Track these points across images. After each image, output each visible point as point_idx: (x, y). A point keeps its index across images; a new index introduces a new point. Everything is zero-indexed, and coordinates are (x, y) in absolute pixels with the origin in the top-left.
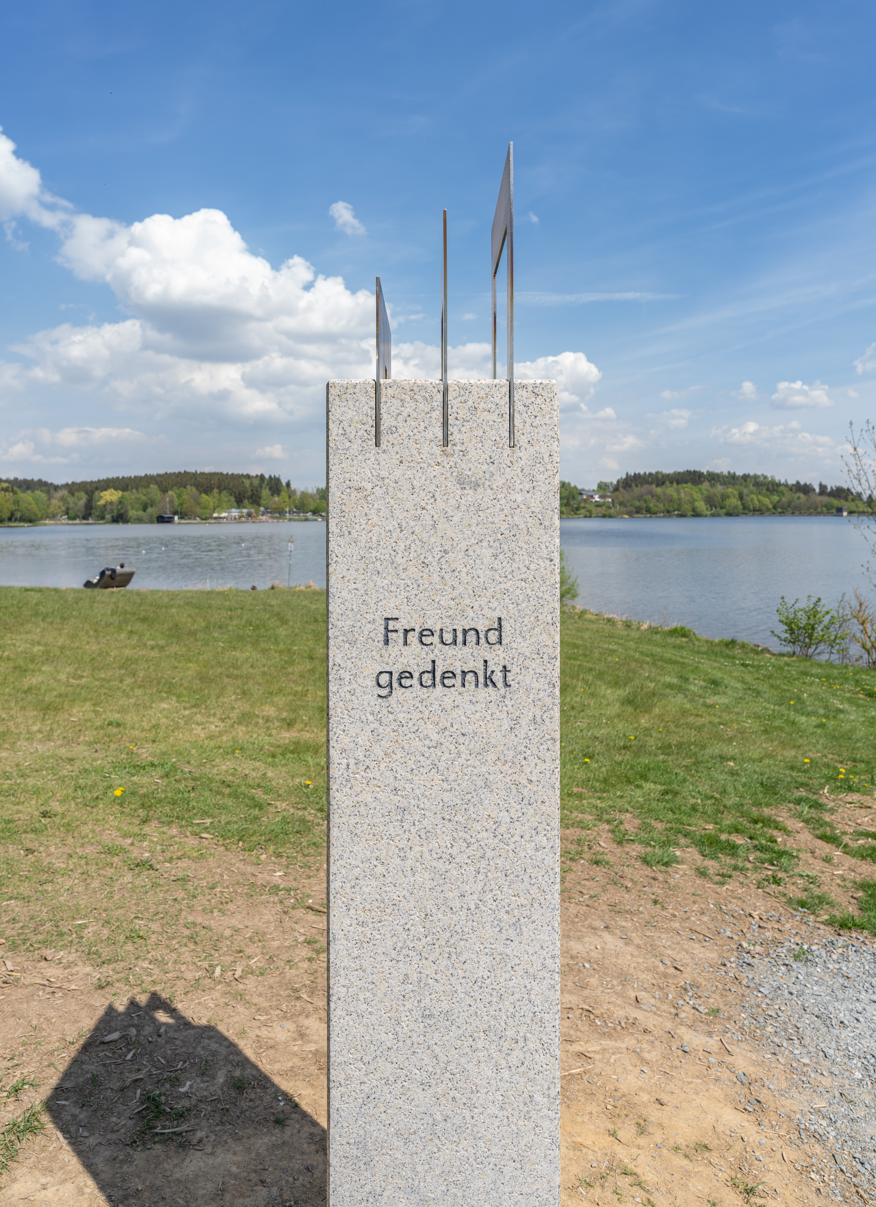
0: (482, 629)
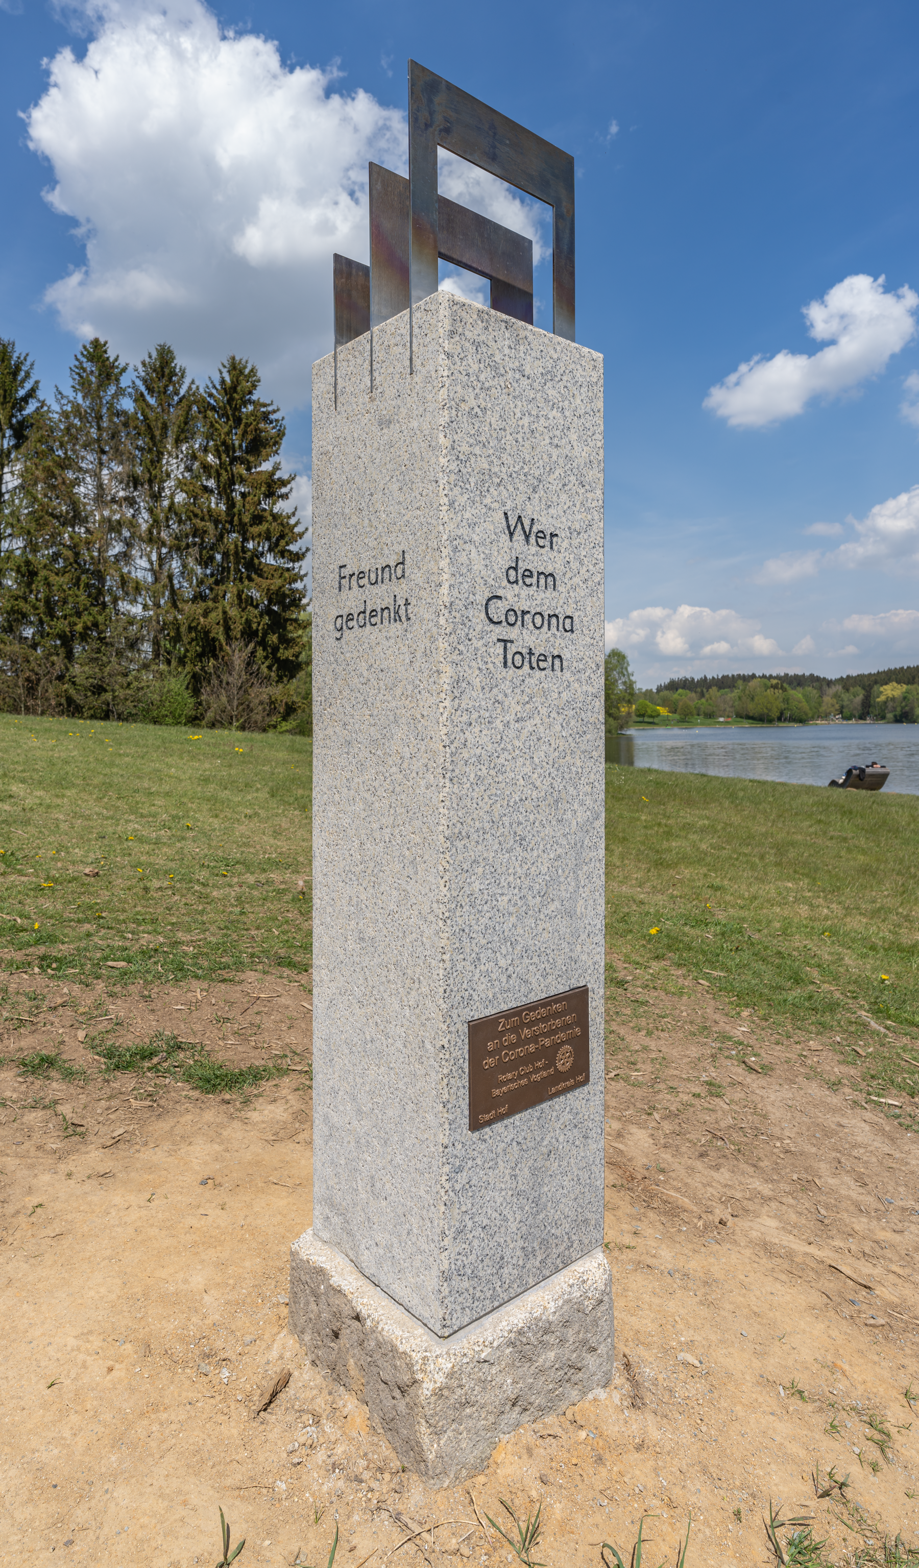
0: (392, 564)
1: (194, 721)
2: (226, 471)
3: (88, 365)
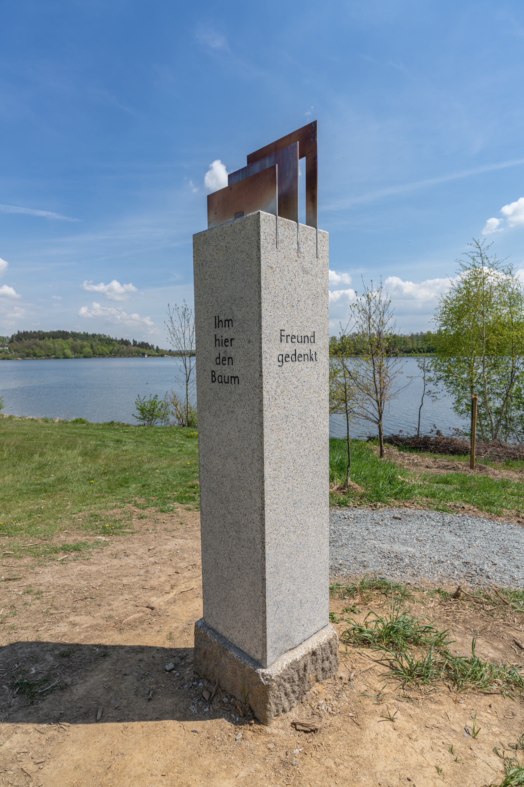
0: (309, 336)
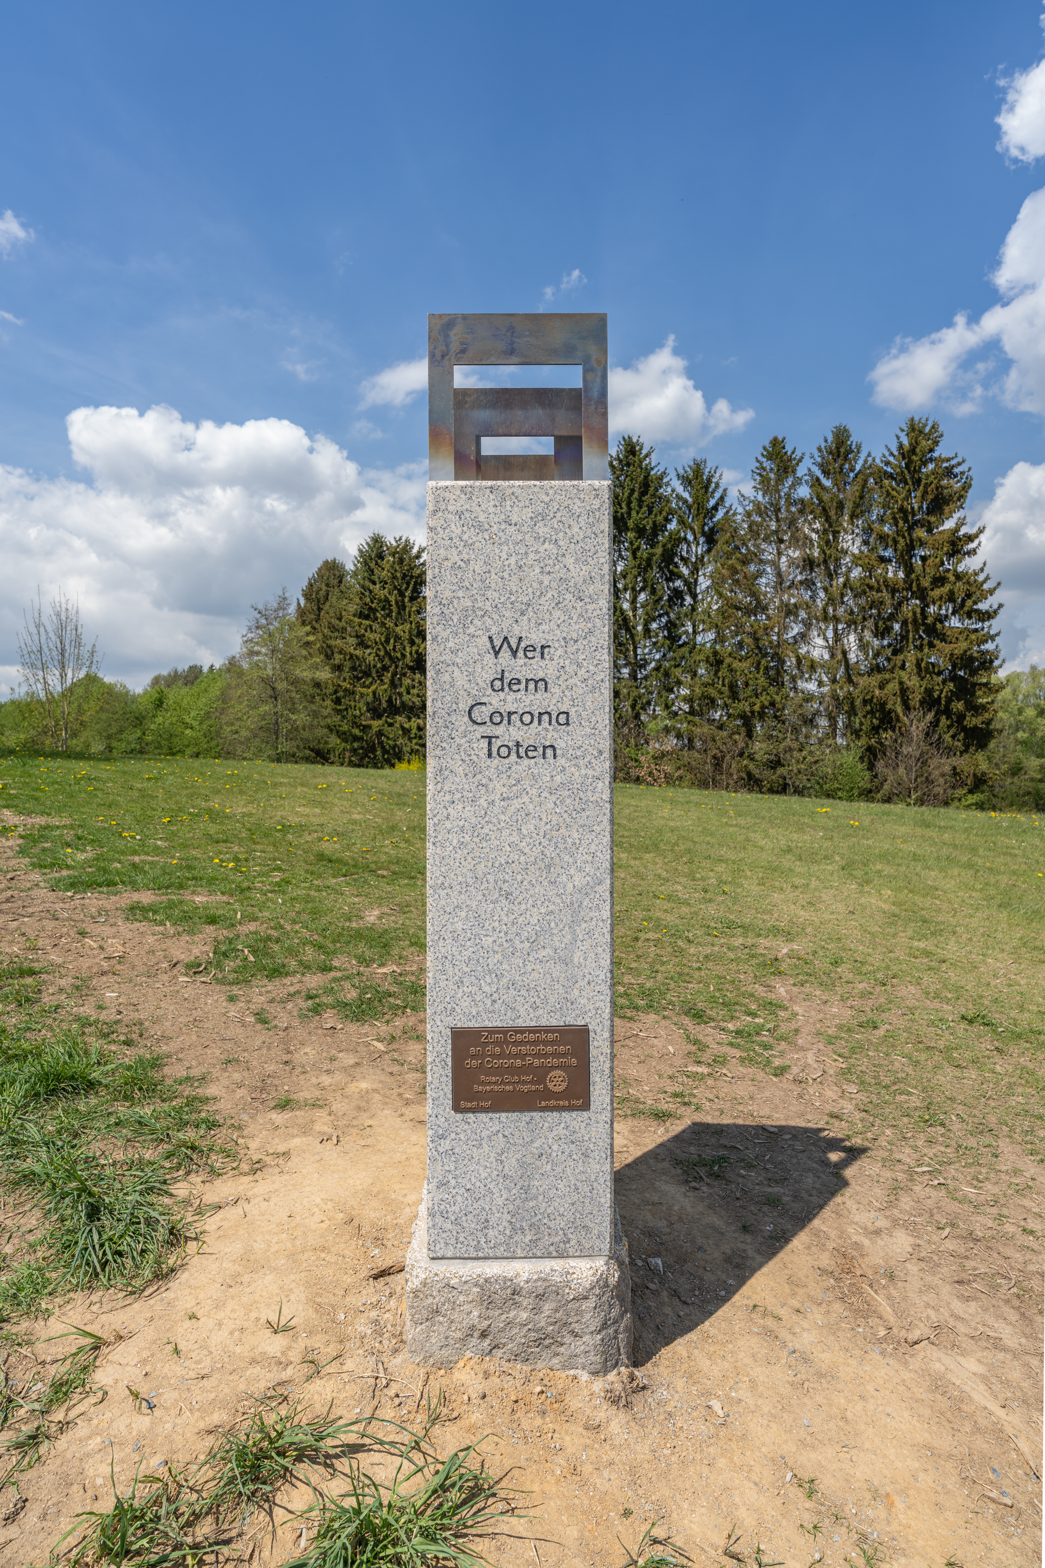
1: (868, 795)
2: (904, 537)
3: (767, 464)
